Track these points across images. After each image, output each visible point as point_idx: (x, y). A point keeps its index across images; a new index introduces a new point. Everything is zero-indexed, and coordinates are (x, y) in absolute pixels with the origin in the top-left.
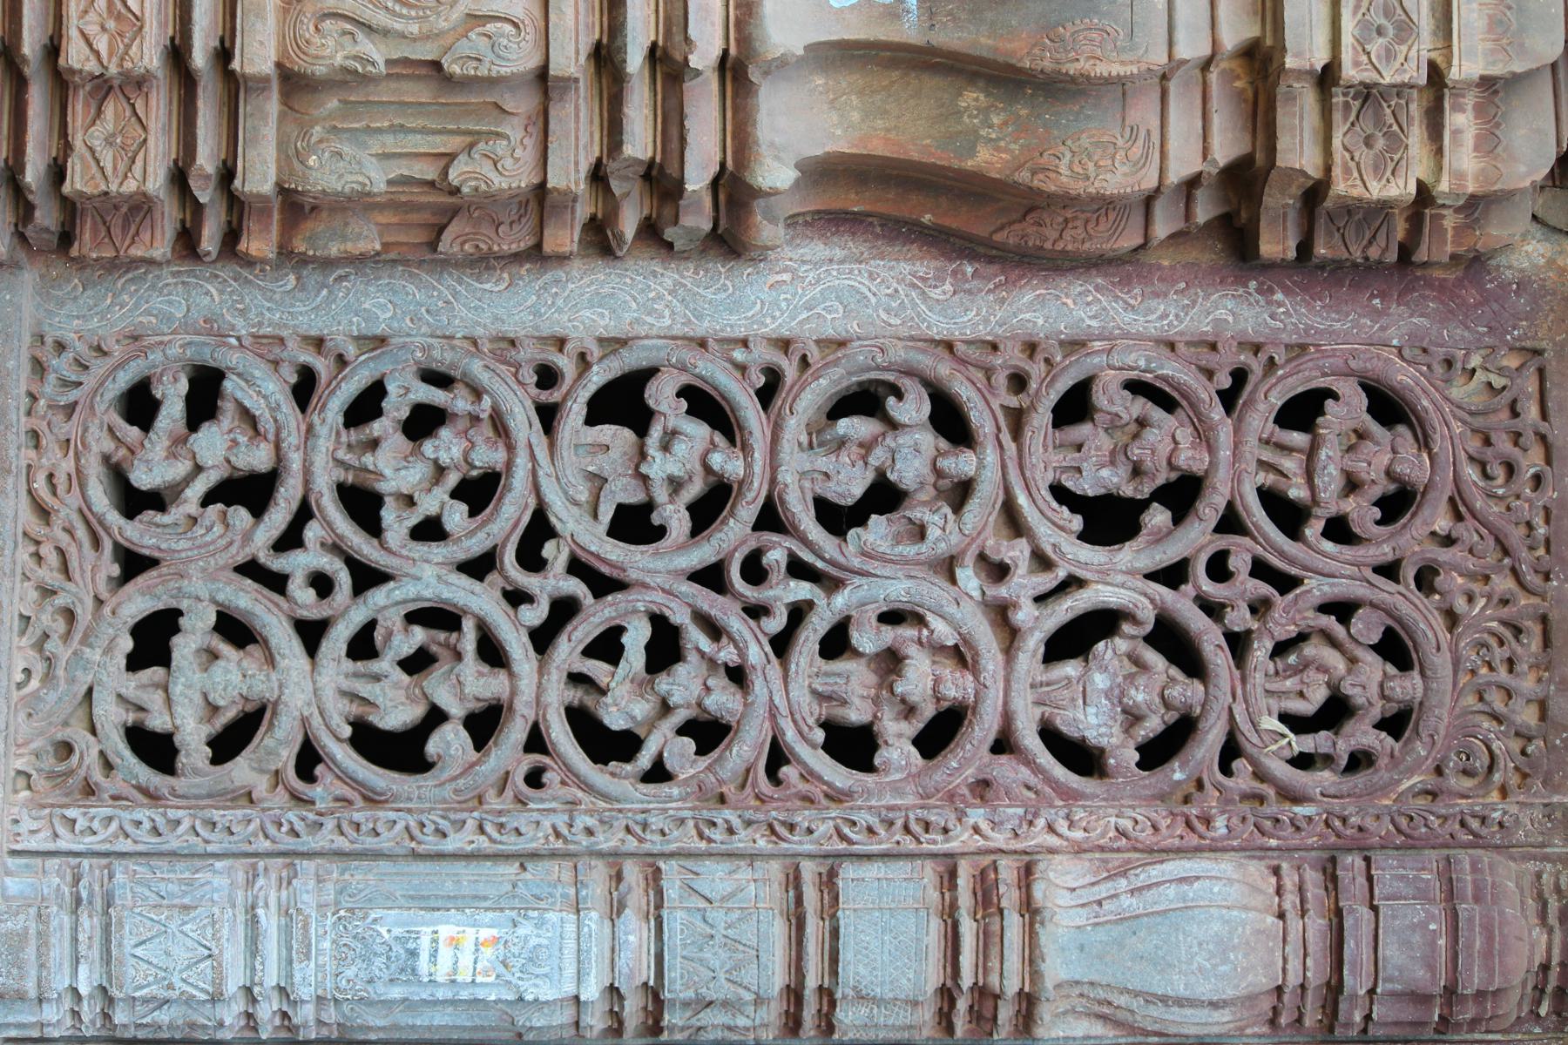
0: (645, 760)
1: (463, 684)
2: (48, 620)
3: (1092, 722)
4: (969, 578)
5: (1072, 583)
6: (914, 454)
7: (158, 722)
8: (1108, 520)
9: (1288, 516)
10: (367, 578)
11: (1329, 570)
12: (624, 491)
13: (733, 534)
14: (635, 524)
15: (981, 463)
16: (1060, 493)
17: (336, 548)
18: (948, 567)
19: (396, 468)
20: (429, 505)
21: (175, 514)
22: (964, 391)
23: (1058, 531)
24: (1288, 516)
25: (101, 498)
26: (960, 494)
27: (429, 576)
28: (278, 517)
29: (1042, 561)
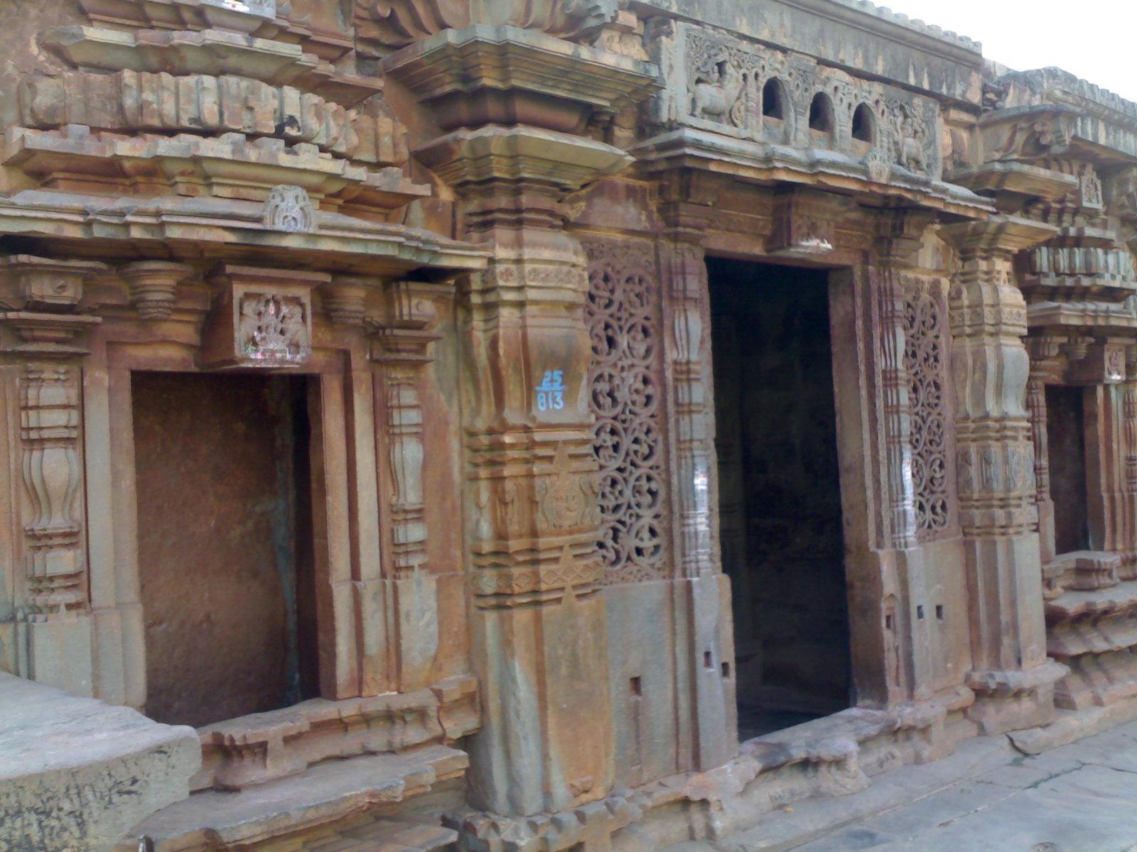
0: (653, 444)
1: (644, 485)
2: (639, 576)
3: (641, 348)
4: (624, 374)
5: (624, 352)
6: (604, 387)
7: (652, 549)
8: (611, 342)
9: (610, 303)
10: (629, 507)
11: (618, 296)
12: (611, 451)
13: (619, 426)
14: (616, 448)
15: (606, 372)
16: (609, 354)
17: (625, 514)
18: (623, 379)
19: (611, 503)
20: (617, 493)
21: (621, 549)
22: (596, 375)
23: (615, 354)
24: (610, 303)
25: (618, 567)
26: (611, 376)
27: (628, 492)
28: (620, 526)
29: (620, 359)
